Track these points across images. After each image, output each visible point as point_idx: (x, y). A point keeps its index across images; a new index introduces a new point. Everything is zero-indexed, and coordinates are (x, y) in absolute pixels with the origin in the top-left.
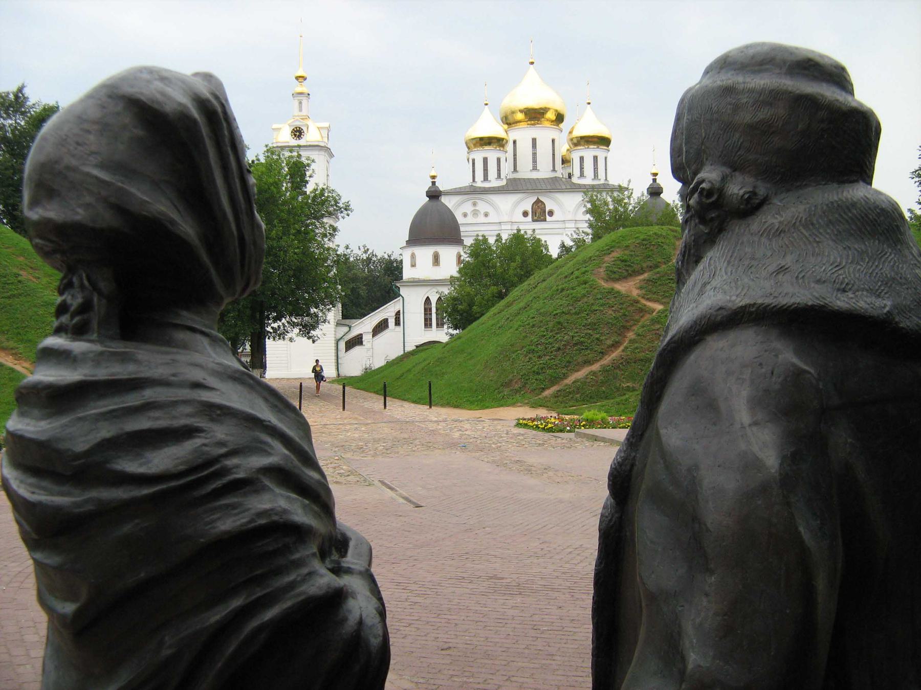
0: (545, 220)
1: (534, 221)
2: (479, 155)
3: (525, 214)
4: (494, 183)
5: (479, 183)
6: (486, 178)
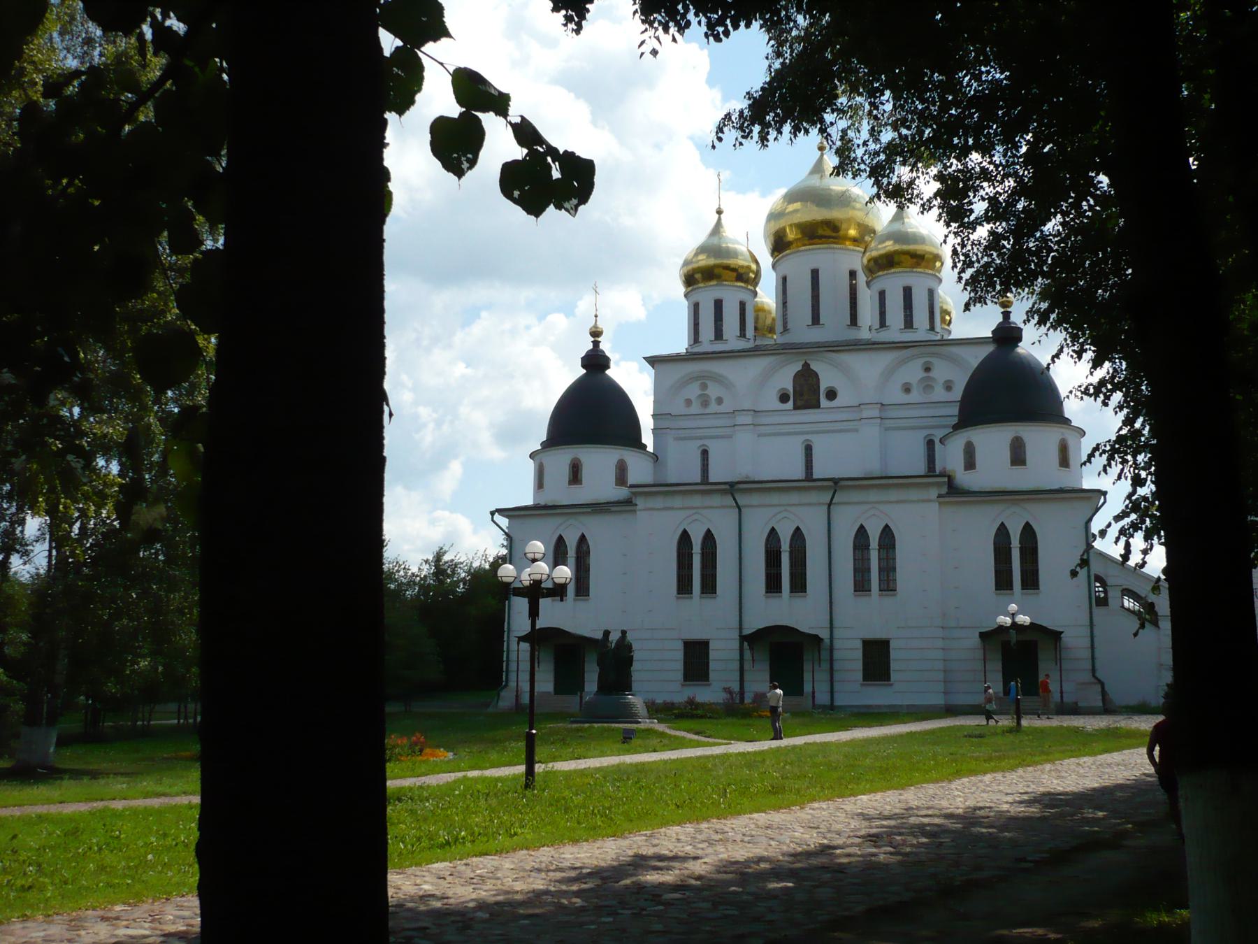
0: (817, 406)
1: (796, 407)
2: (707, 295)
3: (784, 398)
4: (732, 340)
5: (707, 345)
6: (719, 335)
